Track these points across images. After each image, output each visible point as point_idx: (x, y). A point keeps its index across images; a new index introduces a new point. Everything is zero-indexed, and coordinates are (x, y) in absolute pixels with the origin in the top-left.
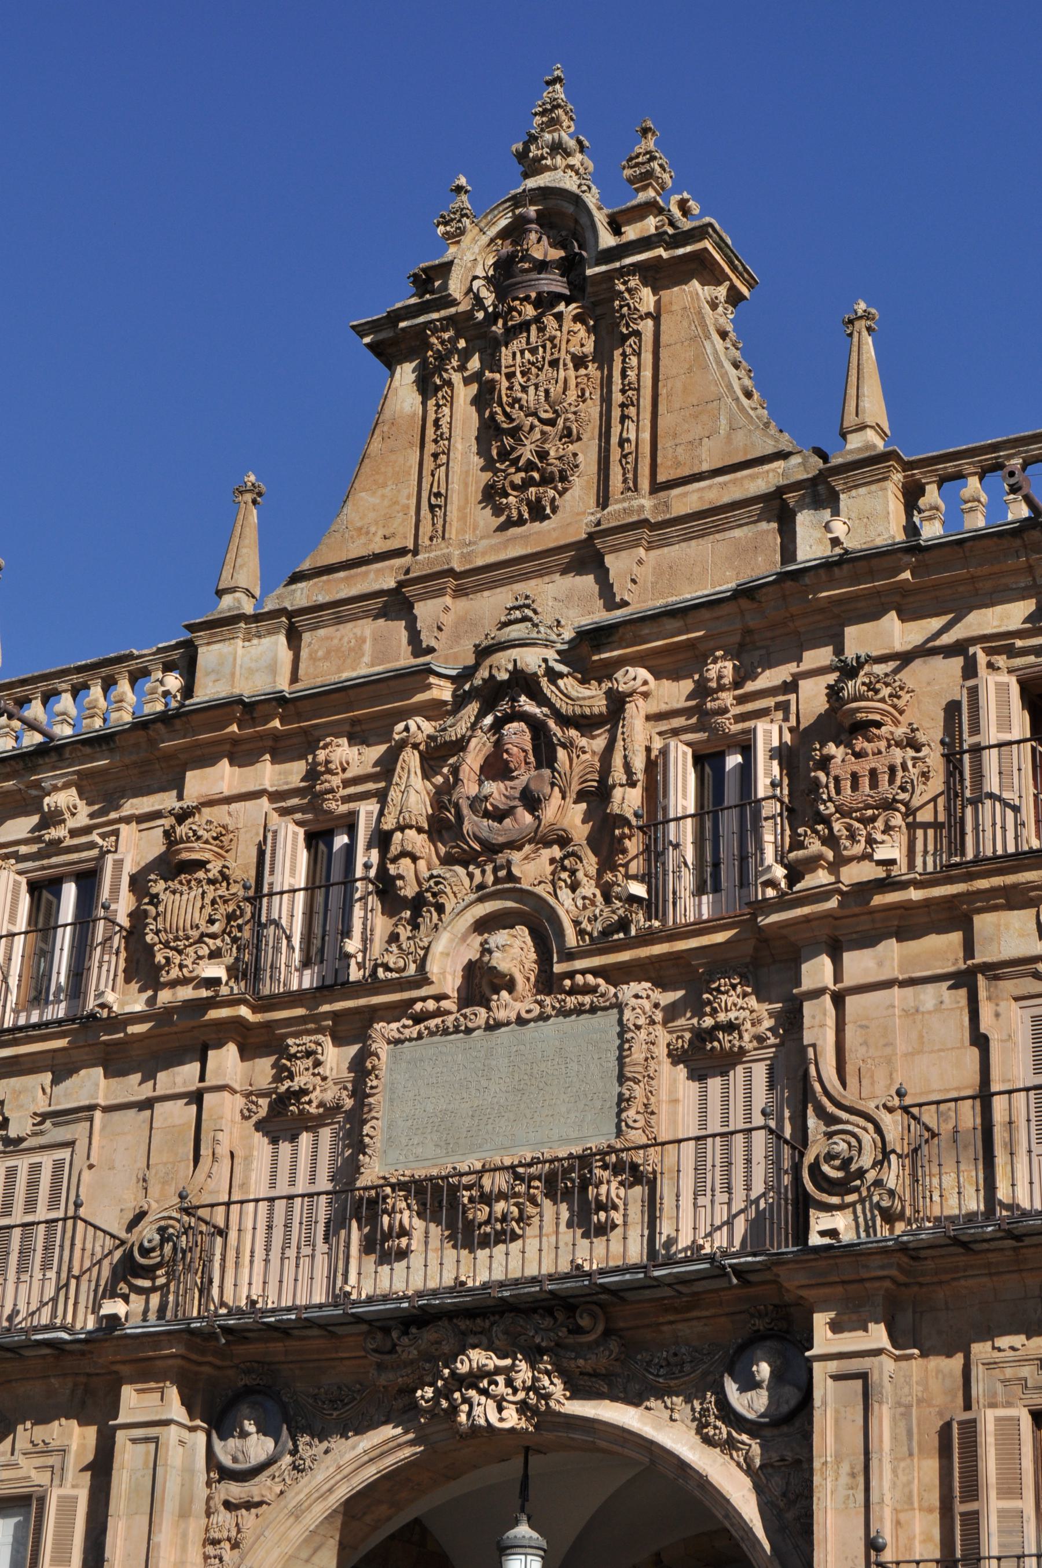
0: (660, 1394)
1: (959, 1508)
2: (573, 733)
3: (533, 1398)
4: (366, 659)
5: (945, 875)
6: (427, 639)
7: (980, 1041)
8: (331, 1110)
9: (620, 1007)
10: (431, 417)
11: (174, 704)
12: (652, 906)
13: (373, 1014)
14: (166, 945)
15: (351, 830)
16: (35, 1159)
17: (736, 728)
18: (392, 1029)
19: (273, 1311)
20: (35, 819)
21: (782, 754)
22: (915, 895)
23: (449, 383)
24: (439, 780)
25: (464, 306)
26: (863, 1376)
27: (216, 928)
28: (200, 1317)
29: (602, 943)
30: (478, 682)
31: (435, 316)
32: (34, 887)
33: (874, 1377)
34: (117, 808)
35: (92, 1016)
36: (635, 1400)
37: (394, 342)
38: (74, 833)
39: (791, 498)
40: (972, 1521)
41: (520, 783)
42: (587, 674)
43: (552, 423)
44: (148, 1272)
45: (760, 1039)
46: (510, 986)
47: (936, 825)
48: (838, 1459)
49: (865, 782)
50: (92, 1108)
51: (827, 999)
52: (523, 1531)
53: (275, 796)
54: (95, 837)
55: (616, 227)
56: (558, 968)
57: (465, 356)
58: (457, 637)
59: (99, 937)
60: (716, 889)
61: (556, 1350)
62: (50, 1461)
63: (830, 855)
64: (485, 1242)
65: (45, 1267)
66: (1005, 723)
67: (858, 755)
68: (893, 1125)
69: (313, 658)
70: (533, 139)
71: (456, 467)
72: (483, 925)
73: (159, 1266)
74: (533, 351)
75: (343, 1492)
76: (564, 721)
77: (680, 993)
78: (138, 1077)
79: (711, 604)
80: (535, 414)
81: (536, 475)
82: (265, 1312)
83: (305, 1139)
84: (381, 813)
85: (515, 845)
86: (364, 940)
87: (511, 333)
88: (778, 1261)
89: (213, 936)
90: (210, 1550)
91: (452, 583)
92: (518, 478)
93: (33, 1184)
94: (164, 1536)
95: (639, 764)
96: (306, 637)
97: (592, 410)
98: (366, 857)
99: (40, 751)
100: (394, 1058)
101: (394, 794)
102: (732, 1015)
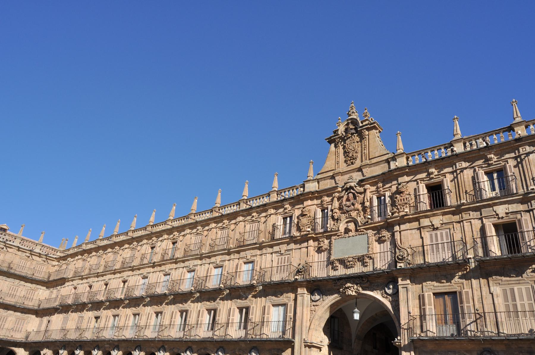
0: (376, 290)
1: (422, 307)
2: (359, 195)
3: (357, 291)
4: (329, 185)
5: (415, 213)
6: (337, 182)
7: (422, 238)
8: (326, 249)
9: (367, 234)
10: (337, 151)
11: (302, 192)
12: (371, 219)
13: (331, 235)
14: (302, 226)
15: (327, 209)
16: (285, 256)
17: (383, 193)
18: (334, 237)
19: (319, 278)
20: (283, 209)
21: (390, 197)
22: (411, 217)
23: (339, 146)
24: (340, 202)
25: (341, 135)
26: (406, 288)
27: (309, 224)
28: (309, 279)
29: (364, 224)
30: (345, 188)
31: (337, 137)
32: (284, 218)
33: (408, 288)
34: (295, 207)
35: (292, 236)
36: (372, 291)
37: (331, 141)
38: (289, 211)
39: (389, 160)
40: (424, 309)
41: (351, 202)
42: (361, 186)
43: (354, 151)
44: (301, 272)
45: (388, 238)
46: (351, 231)
47: (414, 206)
48: (403, 300)
49: (403, 200)
50: (292, 249)
51: (398, 232)
52: (356, 310)
53: (317, 205)
54: (292, 211)
55: (362, 123)
56: (358, 228)
57: (341, 142)
58: (341, 182)
59: (293, 225)
60: (381, 216)
61: (360, 284)
62: (288, 299)
63: (398, 211)
64: (349, 268)
65: (287, 271)
66: (423, 191)
67: (401, 196)
68: (409, 250)
69: (321, 185)
70: (349, 111)
71: (340, 158)
72: (347, 222)
73: (303, 271)
74: (351, 141)
75: (330, 304)
76: (358, 193)
77: (376, 232)
78: (299, 245)
79: (378, 175)
80: (351, 150)
81: (352, 158)
82: (318, 278)
83: (323, 253)
84: (332, 207)
85: (351, 211)
86: (330, 225)
87: (348, 139)
88: (393, 270)
89: (309, 225)
90: (311, 312)
91: (340, 174)
92: (349, 159)
93: (285, 260)
94: (305, 310)
95: (369, 199)
96: (320, 182)
97: (360, 149)
98: (330, 213)
99: (284, 200)
100: (334, 241)
101: (333, 204)
102: (384, 235)
